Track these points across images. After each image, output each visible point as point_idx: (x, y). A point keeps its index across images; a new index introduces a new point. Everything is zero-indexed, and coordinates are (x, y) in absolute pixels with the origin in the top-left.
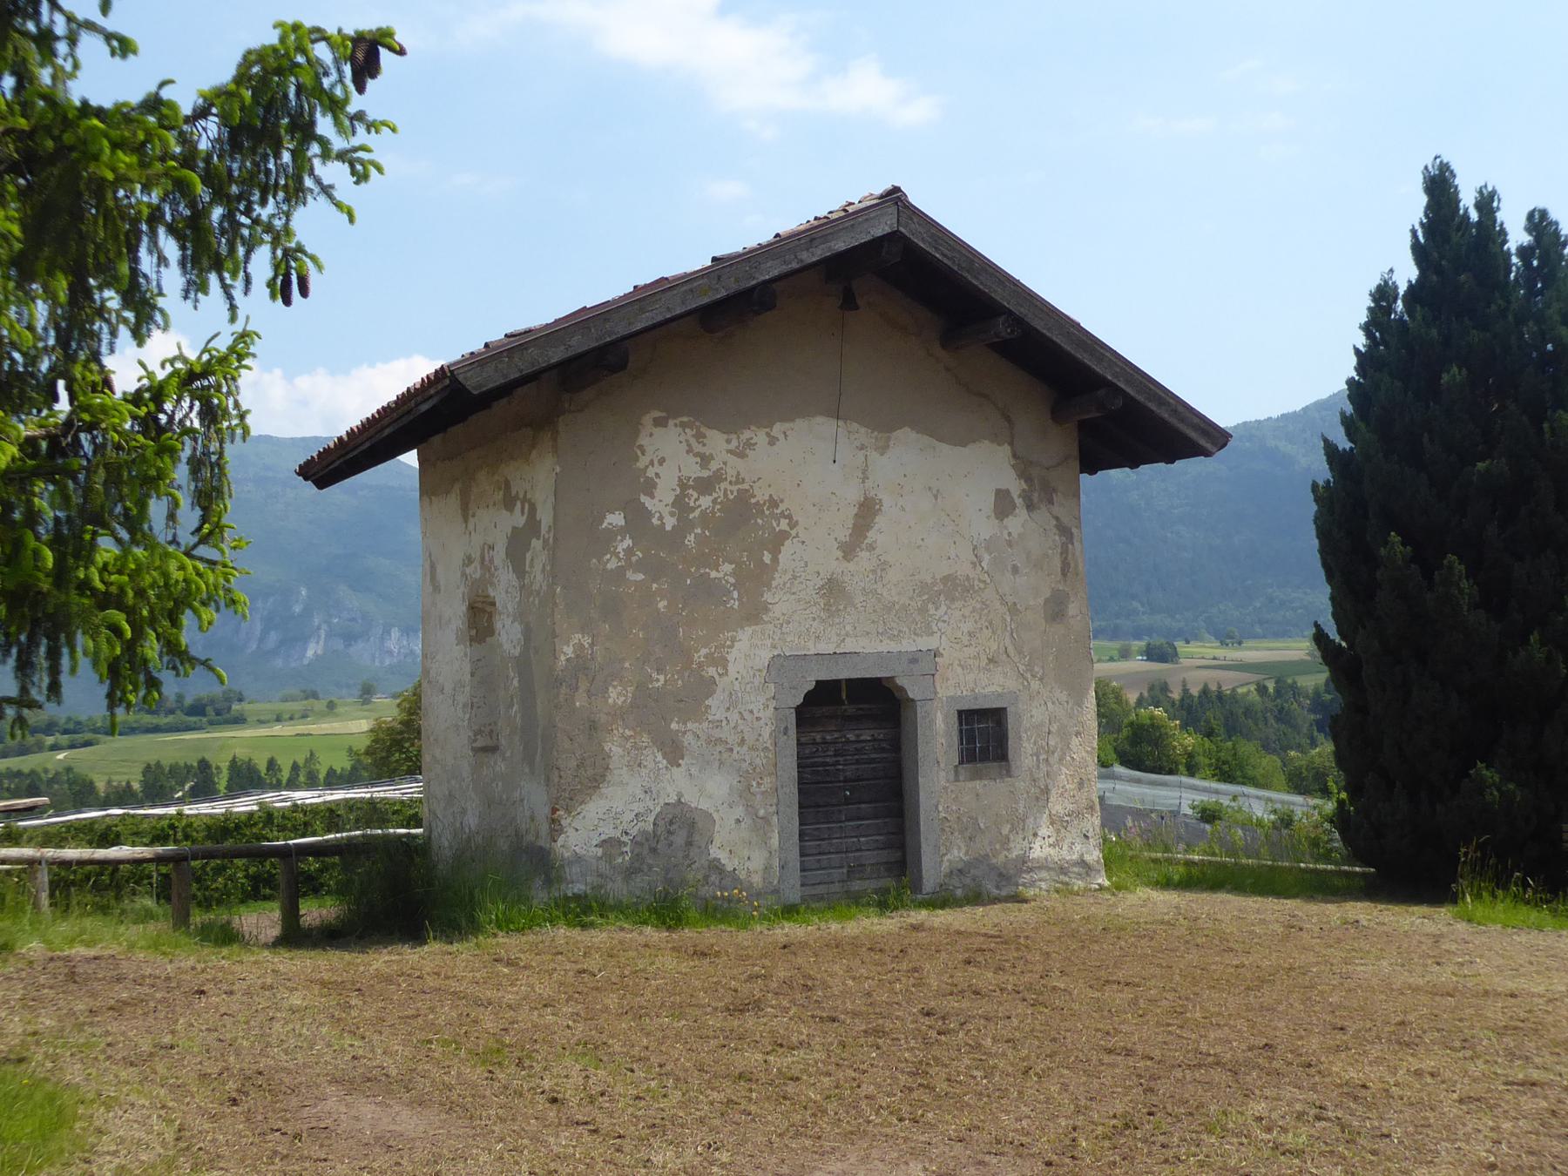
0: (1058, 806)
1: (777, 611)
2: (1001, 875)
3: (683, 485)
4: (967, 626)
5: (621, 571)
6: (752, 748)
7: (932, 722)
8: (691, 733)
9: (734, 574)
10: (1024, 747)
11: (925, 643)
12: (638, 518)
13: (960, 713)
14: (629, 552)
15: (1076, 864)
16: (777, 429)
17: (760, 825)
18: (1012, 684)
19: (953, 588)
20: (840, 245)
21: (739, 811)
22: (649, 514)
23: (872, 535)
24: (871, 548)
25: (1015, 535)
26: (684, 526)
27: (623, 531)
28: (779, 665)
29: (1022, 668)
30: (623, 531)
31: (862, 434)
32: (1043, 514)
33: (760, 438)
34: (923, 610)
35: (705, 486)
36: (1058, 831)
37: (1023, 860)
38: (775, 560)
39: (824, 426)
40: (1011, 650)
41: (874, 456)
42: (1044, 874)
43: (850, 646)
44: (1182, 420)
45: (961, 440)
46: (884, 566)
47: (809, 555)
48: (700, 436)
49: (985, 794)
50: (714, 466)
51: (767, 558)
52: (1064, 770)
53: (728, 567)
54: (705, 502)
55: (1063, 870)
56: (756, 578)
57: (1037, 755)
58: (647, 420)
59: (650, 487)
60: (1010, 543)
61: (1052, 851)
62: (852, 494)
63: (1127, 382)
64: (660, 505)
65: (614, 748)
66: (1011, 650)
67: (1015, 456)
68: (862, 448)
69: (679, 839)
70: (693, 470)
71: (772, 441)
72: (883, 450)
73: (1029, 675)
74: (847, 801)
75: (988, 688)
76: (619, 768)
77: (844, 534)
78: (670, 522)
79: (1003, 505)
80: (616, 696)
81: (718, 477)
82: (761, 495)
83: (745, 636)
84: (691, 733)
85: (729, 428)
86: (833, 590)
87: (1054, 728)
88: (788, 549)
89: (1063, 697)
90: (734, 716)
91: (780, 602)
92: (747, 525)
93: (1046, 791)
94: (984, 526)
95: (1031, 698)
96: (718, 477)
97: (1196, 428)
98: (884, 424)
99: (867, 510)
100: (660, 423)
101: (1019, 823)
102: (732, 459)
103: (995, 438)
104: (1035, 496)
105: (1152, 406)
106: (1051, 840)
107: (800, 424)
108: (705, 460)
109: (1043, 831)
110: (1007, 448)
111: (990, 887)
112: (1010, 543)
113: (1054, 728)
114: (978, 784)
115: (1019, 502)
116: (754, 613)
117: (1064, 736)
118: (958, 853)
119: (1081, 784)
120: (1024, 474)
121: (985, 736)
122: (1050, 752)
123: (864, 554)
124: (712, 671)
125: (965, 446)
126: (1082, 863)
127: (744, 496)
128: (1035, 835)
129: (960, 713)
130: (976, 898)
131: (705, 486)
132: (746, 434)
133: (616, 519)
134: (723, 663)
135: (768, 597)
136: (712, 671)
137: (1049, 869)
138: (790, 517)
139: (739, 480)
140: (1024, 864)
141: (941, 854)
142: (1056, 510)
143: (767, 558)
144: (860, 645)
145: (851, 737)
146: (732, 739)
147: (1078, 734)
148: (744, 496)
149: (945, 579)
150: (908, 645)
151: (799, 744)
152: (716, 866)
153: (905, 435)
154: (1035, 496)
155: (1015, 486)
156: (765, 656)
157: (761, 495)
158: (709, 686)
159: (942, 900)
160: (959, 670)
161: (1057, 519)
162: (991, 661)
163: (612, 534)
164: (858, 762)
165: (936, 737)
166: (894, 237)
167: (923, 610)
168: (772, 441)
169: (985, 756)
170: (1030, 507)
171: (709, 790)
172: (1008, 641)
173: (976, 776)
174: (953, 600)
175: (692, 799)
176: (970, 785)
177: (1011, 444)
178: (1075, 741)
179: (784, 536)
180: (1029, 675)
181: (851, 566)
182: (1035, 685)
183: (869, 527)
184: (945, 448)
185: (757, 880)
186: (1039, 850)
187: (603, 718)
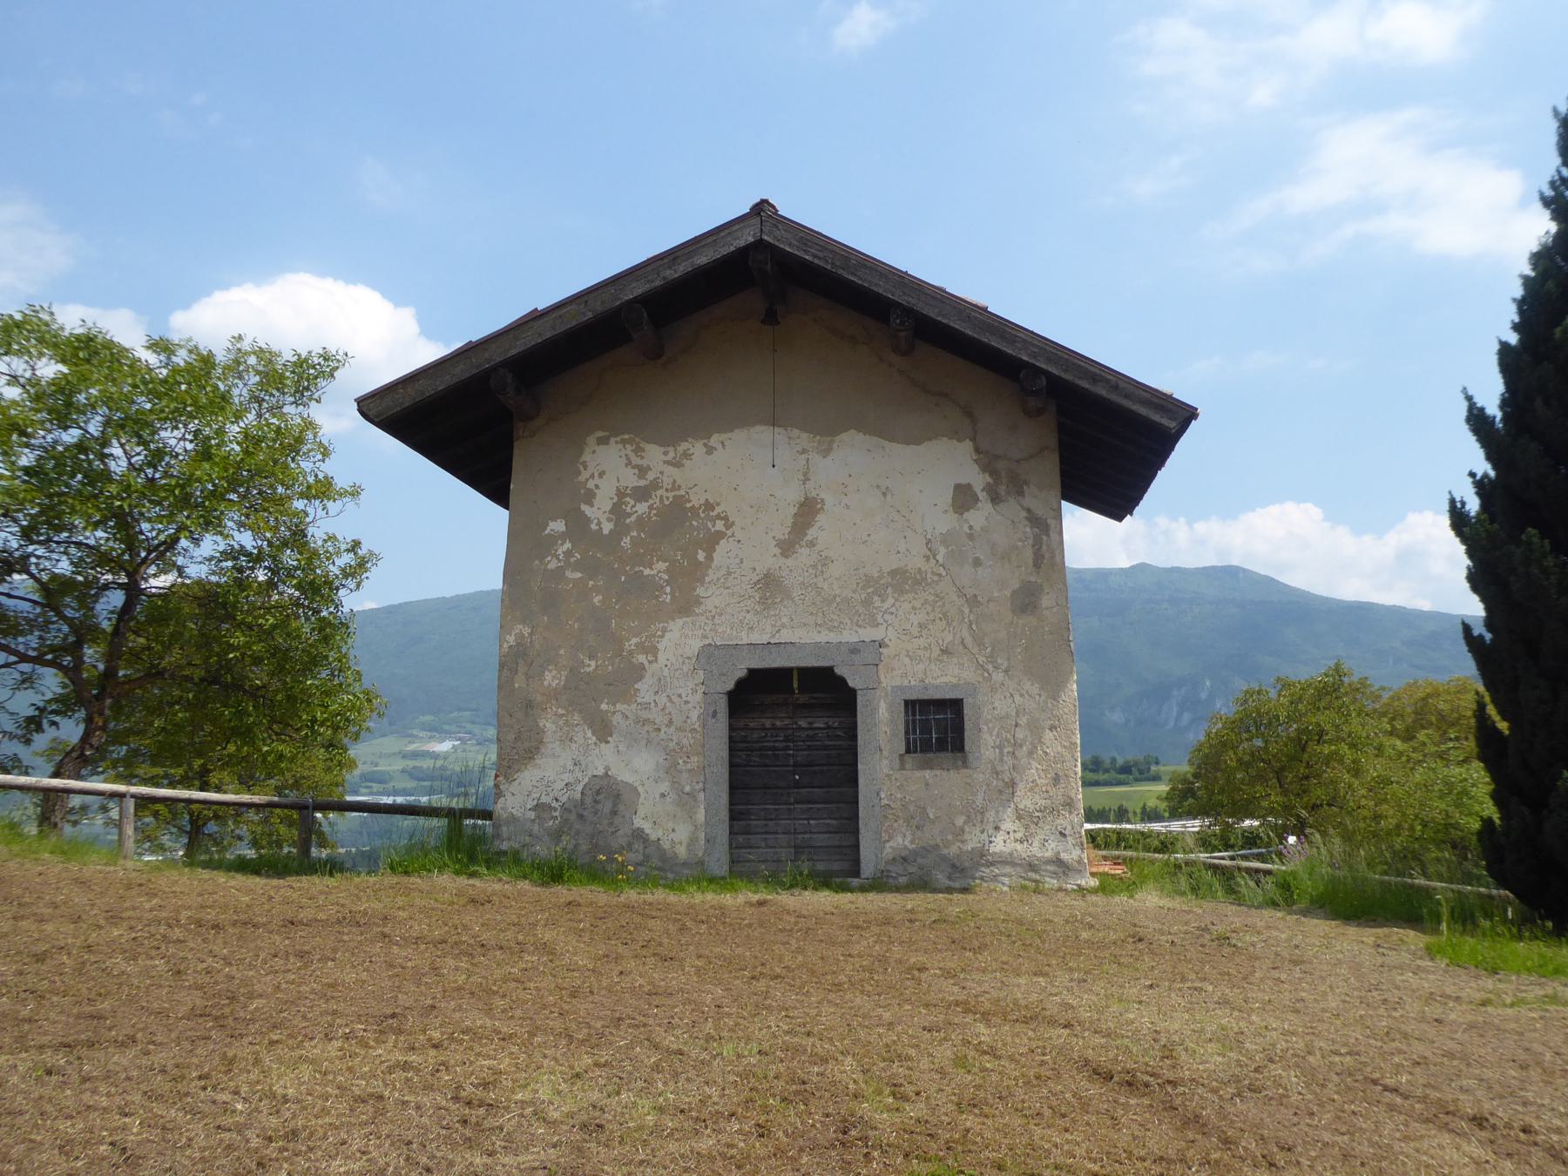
1: (709, 604)
2: (953, 866)
3: (621, 494)
4: (915, 619)
6: (680, 729)
7: (875, 710)
9: (667, 571)
10: (984, 740)
11: (868, 634)
12: (578, 526)
13: (907, 702)
14: (568, 553)
15: (1049, 862)
16: (715, 440)
17: (685, 801)
18: (969, 675)
19: (902, 581)
21: (664, 787)
22: (588, 520)
23: (812, 533)
24: (812, 544)
25: (977, 528)
26: (620, 530)
27: (563, 537)
28: (708, 654)
29: (981, 659)
30: (563, 537)
31: (804, 439)
32: (1012, 508)
33: (697, 448)
34: (867, 603)
35: (642, 494)
36: (1027, 827)
38: (710, 558)
39: (763, 433)
40: (969, 640)
41: (816, 458)
42: (1008, 869)
43: (785, 636)
45: (917, 441)
46: (825, 561)
47: (746, 551)
48: (638, 451)
49: (937, 783)
50: (651, 476)
51: (701, 556)
52: (1035, 764)
53: (662, 566)
54: (642, 508)
55: (1032, 867)
56: (689, 575)
57: (1001, 747)
58: (591, 440)
59: (590, 497)
60: (971, 537)
61: (1019, 847)
62: (792, 495)
63: (1049, 360)
64: (598, 514)
65: (548, 724)
66: (969, 640)
67: (977, 450)
68: (804, 451)
69: (607, 807)
70: (631, 479)
71: (710, 450)
72: (826, 453)
73: (990, 667)
74: (797, 785)
75: (942, 678)
76: (552, 744)
77: (782, 532)
78: (607, 527)
79: (963, 498)
80: (552, 679)
81: (655, 485)
82: (696, 500)
83: (676, 627)
84: (620, 713)
85: (668, 440)
86: (769, 586)
87: (1023, 721)
88: (722, 547)
89: (1035, 689)
90: (662, 700)
91: (712, 596)
92: (684, 530)
93: (1012, 784)
94: (942, 521)
95: (993, 690)
96: (655, 485)
98: (826, 429)
99: (808, 510)
100: (603, 441)
101: (976, 815)
102: (669, 470)
103: (956, 435)
104: (1002, 489)
105: (1084, 384)
106: (1019, 835)
107: (739, 435)
108: (642, 471)
109: (1008, 825)
110: (968, 445)
111: (941, 878)
112: (971, 537)
113: (1023, 721)
114: (927, 774)
115: (982, 495)
116: (686, 606)
117: (1035, 729)
118: (902, 841)
119: (1056, 780)
121: (938, 727)
122: (1017, 745)
123: (804, 551)
124: (642, 658)
125: (917, 442)
126: (1058, 862)
127: (679, 502)
128: (997, 828)
129: (907, 702)
130: (922, 884)
131: (642, 494)
132: (684, 446)
133: (558, 526)
134: (653, 651)
135: (700, 591)
136: (642, 658)
137: (1013, 864)
138: (726, 519)
139: (675, 487)
140: (981, 857)
141: (882, 840)
142: (1028, 501)
143: (701, 556)
144: (797, 635)
145: (803, 723)
147: (1052, 728)
148: (679, 502)
149: (893, 573)
150: (849, 636)
152: (639, 835)
154: (1002, 489)
155: (978, 480)
156: (695, 645)
157: (696, 500)
159: (879, 884)
160: (907, 660)
161: (1029, 510)
162: (944, 652)
163: (555, 539)
164: (809, 748)
165: (880, 726)
166: (759, 244)
167: (867, 603)
168: (710, 450)
170: (995, 499)
171: (635, 766)
172: (965, 633)
173: (926, 765)
174: (902, 592)
175: (623, 775)
176: (918, 774)
177: (973, 439)
178: (1048, 735)
179: (719, 536)
180: (990, 667)
181: (789, 562)
182: (998, 677)
183: (809, 525)
184: (896, 448)
185: (682, 851)
186: (1000, 845)
187: (539, 698)
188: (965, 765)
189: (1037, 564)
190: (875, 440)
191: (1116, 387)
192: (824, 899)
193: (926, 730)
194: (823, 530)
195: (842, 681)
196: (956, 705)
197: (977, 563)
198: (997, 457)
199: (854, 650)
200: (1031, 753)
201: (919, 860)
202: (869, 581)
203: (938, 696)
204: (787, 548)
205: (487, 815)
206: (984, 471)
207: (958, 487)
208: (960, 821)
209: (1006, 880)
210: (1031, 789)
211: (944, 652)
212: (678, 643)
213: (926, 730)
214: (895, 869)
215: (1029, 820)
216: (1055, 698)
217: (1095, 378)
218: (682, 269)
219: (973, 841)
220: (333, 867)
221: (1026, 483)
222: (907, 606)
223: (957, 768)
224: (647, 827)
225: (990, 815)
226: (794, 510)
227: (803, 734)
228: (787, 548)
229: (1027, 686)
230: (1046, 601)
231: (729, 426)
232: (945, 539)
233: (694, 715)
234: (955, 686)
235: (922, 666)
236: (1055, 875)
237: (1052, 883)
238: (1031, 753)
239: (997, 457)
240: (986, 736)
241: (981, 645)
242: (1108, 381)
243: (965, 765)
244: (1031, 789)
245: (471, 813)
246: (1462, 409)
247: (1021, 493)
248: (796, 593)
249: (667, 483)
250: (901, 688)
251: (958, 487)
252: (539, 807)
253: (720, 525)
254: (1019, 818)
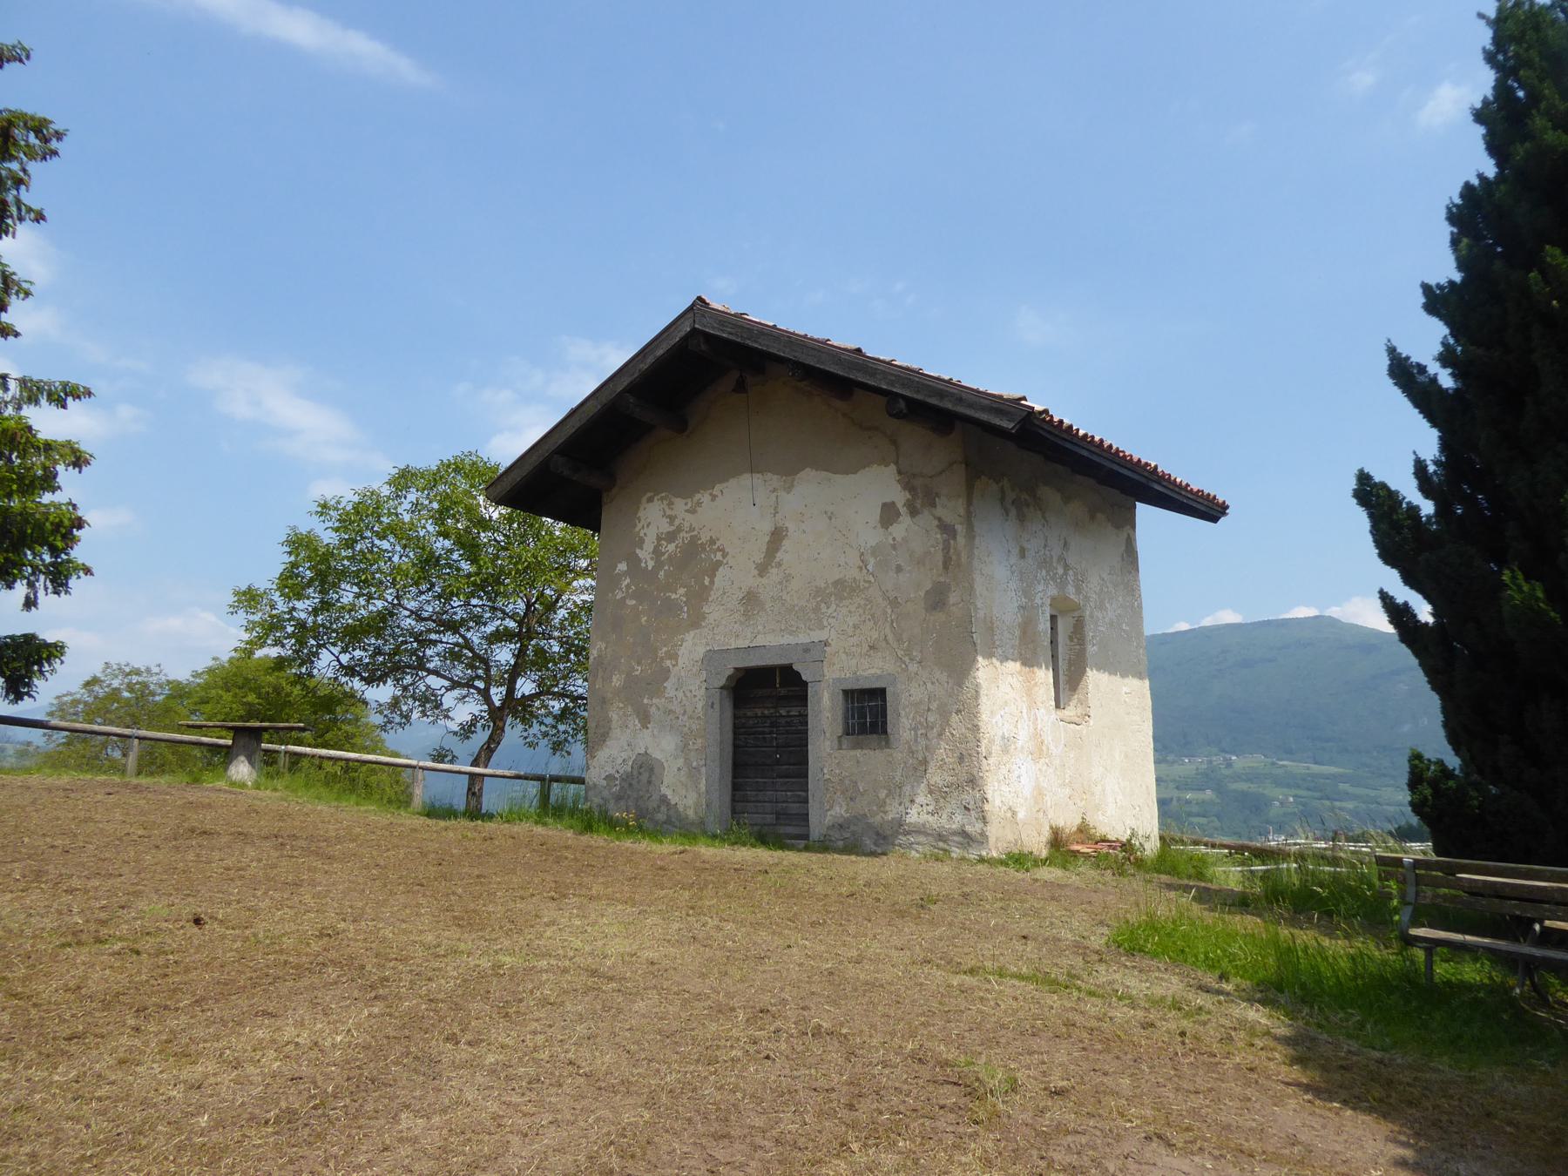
0: (936, 777)
1: (711, 619)
2: (878, 834)
3: (659, 539)
4: (851, 621)
5: (624, 599)
6: (690, 717)
7: (819, 701)
8: (655, 704)
9: (686, 595)
10: (902, 723)
11: (817, 636)
12: (634, 561)
13: (846, 692)
14: (628, 586)
15: (955, 833)
16: (718, 487)
17: (693, 773)
19: (843, 589)
20: (660, 352)
21: (680, 762)
22: (640, 560)
23: (779, 555)
24: (779, 565)
25: (899, 539)
26: (659, 565)
28: (710, 656)
29: (900, 653)
30: (625, 574)
31: (774, 480)
32: (926, 519)
33: (705, 497)
34: (817, 610)
35: (671, 537)
36: (937, 801)
37: (900, 823)
38: (712, 582)
39: (746, 479)
40: (890, 637)
41: (782, 494)
42: (922, 839)
44: (970, 406)
45: (852, 469)
46: (788, 578)
47: (735, 576)
48: (671, 504)
49: (867, 760)
50: (677, 522)
51: (707, 581)
52: (943, 744)
53: (682, 591)
55: (940, 837)
56: (700, 595)
57: (915, 729)
58: (644, 499)
60: (894, 547)
61: (930, 818)
62: (767, 526)
63: (903, 385)
64: (645, 554)
65: (614, 716)
66: (890, 637)
67: (899, 472)
68: (775, 490)
69: (644, 777)
70: (665, 527)
71: (714, 497)
72: (789, 489)
73: (906, 659)
74: (778, 762)
75: (870, 671)
76: (616, 732)
77: (759, 557)
78: (651, 564)
79: (889, 514)
80: (617, 681)
81: (679, 529)
82: (704, 538)
83: (689, 637)
84: (655, 704)
85: (687, 493)
86: (751, 600)
87: (934, 706)
88: (721, 571)
89: (944, 677)
90: (680, 695)
91: (713, 612)
92: (696, 559)
93: (925, 762)
94: (868, 533)
95: (910, 679)
96: (679, 529)
97: (983, 409)
98: (789, 470)
100: (650, 500)
101: (895, 790)
102: (688, 516)
103: (884, 462)
104: (918, 504)
105: (933, 401)
106: (930, 808)
107: (733, 482)
108: (672, 519)
109: (920, 799)
110: (893, 467)
111: (868, 843)
112: (894, 547)
113: (934, 706)
114: (858, 753)
115: (903, 510)
116: (696, 622)
117: (945, 714)
118: (839, 811)
119: (961, 758)
120: (908, 486)
121: (868, 712)
123: (774, 571)
124: (668, 663)
126: (964, 834)
127: (694, 539)
128: (912, 801)
129: (846, 692)
130: (852, 848)
132: (698, 496)
133: (622, 567)
134: (673, 656)
135: (706, 609)
136: (668, 663)
137: (926, 834)
138: (723, 550)
139: (692, 529)
140: (899, 826)
141: (826, 811)
142: (939, 511)
143: (707, 581)
144: (767, 640)
145: (783, 712)
146: (679, 710)
147: (958, 712)
148: (694, 539)
149: (836, 583)
150: (803, 638)
151: (735, 717)
152: (664, 800)
153: (808, 474)
154: (918, 504)
155: (899, 497)
156: (701, 651)
157: (704, 538)
158: (665, 675)
159: (824, 847)
160: (844, 656)
161: (939, 519)
162: (871, 647)
164: (788, 732)
165: (825, 712)
167: (817, 610)
168: (714, 497)
169: (863, 730)
170: (913, 512)
171: (662, 746)
172: (888, 630)
174: (842, 599)
176: (853, 753)
177: (896, 463)
178: (955, 718)
179: (719, 564)
180: (906, 659)
181: (764, 581)
182: (913, 667)
183: (777, 550)
184: (838, 477)
185: (691, 813)
186: (914, 816)
187: (609, 695)
188: (888, 744)
189: (946, 565)
190: (824, 474)
191: (960, 400)
192: (764, 855)
193: (862, 716)
194: (786, 554)
195: (798, 674)
196: (881, 693)
197: (899, 569)
198: (914, 475)
199: (806, 649)
200: (940, 735)
201: (852, 828)
202: (819, 591)
203: (867, 686)
204: (762, 569)
205: (581, 781)
206: (905, 488)
207: (884, 505)
208: (883, 793)
209: (920, 848)
210: (941, 767)
211: (871, 647)
212: (691, 649)
213: (862, 716)
214: (835, 835)
215: (940, 794)
216: (960, 685)
217: (941, 394)
218: (650, 360)
219: (893, 812)
220: (490, 817)
221: (937, 495)
222: (844, 610)
223: (881, 748)
224: (669, 793)
225: (907, 789)
226: (767, 539)
227: (783, 721)
228: (762, 569)
229: (937, 674)
230: (953, 598)
231: (725, 480)
232: (875, 551)
233: (700, 705)
234: (879, 677)
235: (854, 662)
236: (961, 845)
237: (956, 852)
238: (940, 735)
239: (914, 475)
240: (904, 720)
241: (899, 640)
242: (952, 395)
243: (888, 744)
244: (941, 767)
245: (557, 779)
246: (1385, 362)
247: (933, 505)
248: (768, 606)
249: (687, 525)
250: (839, 680)
251: (884, 505)
252: (609, 778)
253: (719, 556)
254: (931, 792)
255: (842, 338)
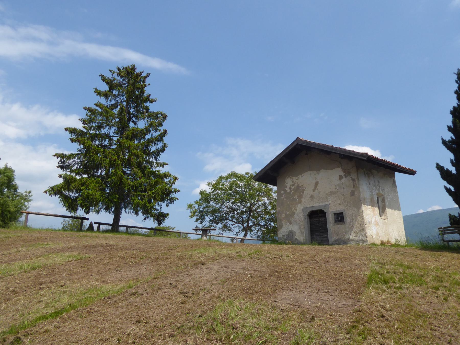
0: (355, 229)
5: (283, 199)
8: (292, 220)
10: (347, 219)
11: (327, 203)
12: (285, 191)
13: (334, 214)
17: (302, 233)
18: (344, 208)
19: (332, 193)
21: (299, 231)
27: (283, 193)
28: (304, 209)
30: (283, 193)
31: (315, 172)
33: (300, 177)
34: (327, 198)
35: (293, 185)
37: (349, 239)
39: (309, 172)
41: (317, 175)
43: (314, 205)
44: (357, 155)
45: (332, 169)
47: (308, 192)
48: (292, 179)
49: (340, 227)
54: (293, 187)
55: (357, 241)
56: (301, 197)
59: (286, 187)
60: (342, 184)
62: (314, 182)
64: (288, 189)
65: (283, 223)
69: (291, 235)
70: (291, 183)
71: (302, 177)
72: (318, 174)
75: (339, 209)
76: (284, 226)
77: (313, 188)
78: (289, 191)
79: (341, 178)
80: (283, 215)
81: (295, 183)
84: (292, 220)
86: (312, 197)
91: (304, 200)
92: (299, 190)
93: (353, 226)
96: (295, 183)
98: (318, 170)
99: (317, 184)
100: (288, 178)
101: (347, 232)
102: (297, 181)
103: (338, 167)
108: (293, 181)
109: (352, 234)
110: (340, 169)
114: (338, 226)
115: (344, 176)
116: (300, 202)
117: (356, 216)
118: (335, 238)
119: (360, 225)
120: (344, 172)
122: (353, 219)
125: (332, 169)
126: (362, 240)
127: (298, 186)
129: (334, 214)
131: (293, 185)
133: (283, 192)
134: (296, 210)
140: (348, 240)
141: (332, 237)
142: (351, 176)
144: (317, 205)
146: (298, 220)
148: (298, 186)
149: (330, 192)
150: (324, 204)
151: (310, 221)
152: (296, 239)
153: (322, 170)
155: (342, 174)
156: (302, 208)
158: (294, 213)
163: (282, 194)
165: (330, 218)
166: (297, 144)
167: (327, 198)
168: (302, 177)
169: (339, 221)
170: (346, 177)
171: (295, 228)
173: (338, 224)
175: (294, 230)
179: (304, 190)
182: (349, 208)
186: (351, 237)
189: (354, 186)
194: (319, 187)
197: (344, 188)
199: (325, 206)
204: (314, 190)
208: (344, 234)
212: (300, 208)
213: (338, 218)
215: (356, 233)
216: (359, 210)
218: (288, 150)
224: (297, 238)
225: (349, 232)
228: (314, 190)
229: (354, 209)
230: (356, 193)
243: (344, 224)
246: (441, 141)
247: (350, 175)
252: (283, 236)
253: (304, 188)
255: (329, 144)
